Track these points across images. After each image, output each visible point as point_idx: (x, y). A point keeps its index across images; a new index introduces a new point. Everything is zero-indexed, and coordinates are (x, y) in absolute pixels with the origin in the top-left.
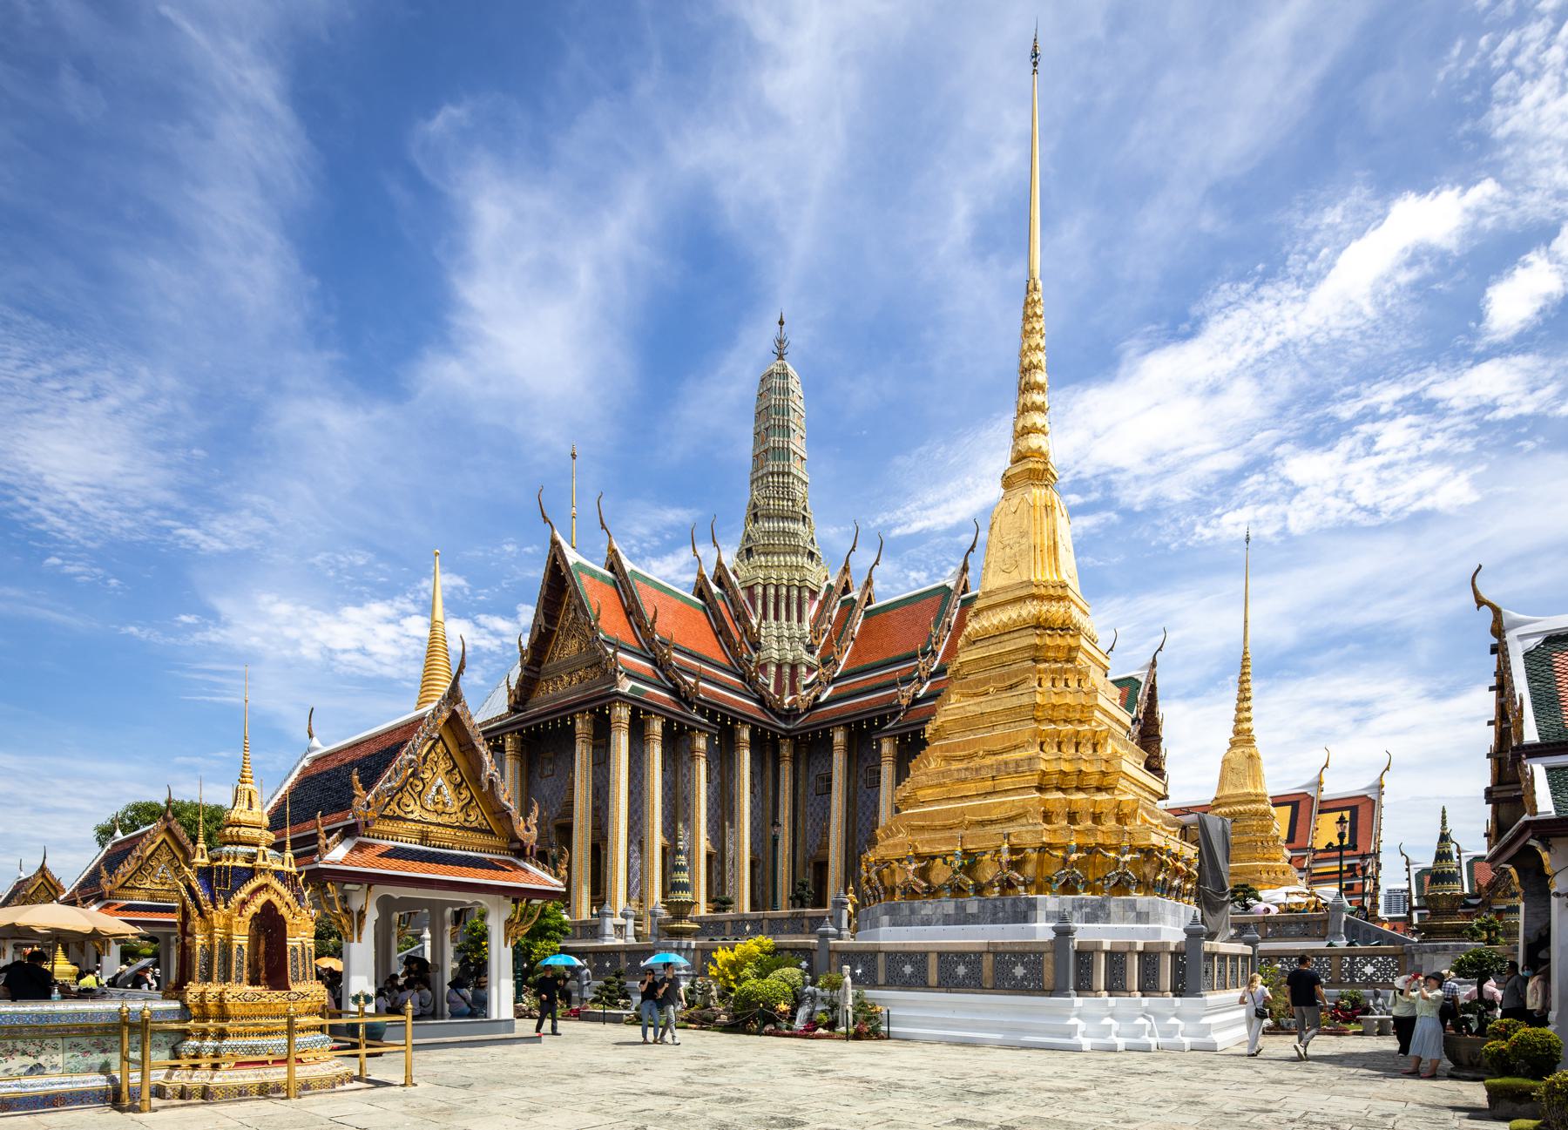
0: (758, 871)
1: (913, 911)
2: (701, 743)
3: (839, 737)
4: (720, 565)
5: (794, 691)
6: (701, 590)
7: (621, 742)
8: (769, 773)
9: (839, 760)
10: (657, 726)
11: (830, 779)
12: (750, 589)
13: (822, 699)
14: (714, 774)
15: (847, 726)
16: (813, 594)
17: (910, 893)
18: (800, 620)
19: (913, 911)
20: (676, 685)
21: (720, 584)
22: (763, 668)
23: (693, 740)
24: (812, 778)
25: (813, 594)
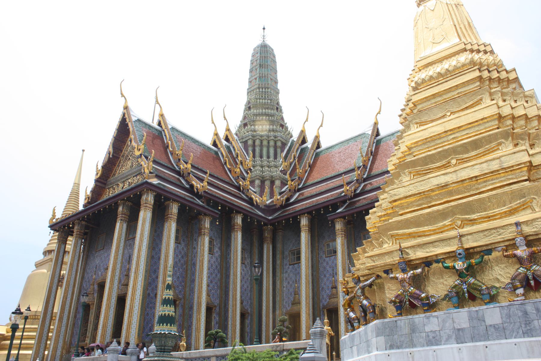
0: (247, 322)
1: (413, 329)
2: (207, 224)
3: (304, 222)
4: (228, 130)
5: (272, 195)
6: (215, 142)
7: (145, 216)
8: (256, 251)
9: (304, 237)
10: (174, 209)
11: (299, 253)
13: (292, 201)
14: (216, 249)
15: (308, 213)
16: (282, 143)
17: (406, 305)
18: (275, 157)
19: (413, 329)
20: (192, 186)
21: (227, 139)
22: (252, 182)
23: (200, 221)
24: (286, 253)
25: (284, 145)
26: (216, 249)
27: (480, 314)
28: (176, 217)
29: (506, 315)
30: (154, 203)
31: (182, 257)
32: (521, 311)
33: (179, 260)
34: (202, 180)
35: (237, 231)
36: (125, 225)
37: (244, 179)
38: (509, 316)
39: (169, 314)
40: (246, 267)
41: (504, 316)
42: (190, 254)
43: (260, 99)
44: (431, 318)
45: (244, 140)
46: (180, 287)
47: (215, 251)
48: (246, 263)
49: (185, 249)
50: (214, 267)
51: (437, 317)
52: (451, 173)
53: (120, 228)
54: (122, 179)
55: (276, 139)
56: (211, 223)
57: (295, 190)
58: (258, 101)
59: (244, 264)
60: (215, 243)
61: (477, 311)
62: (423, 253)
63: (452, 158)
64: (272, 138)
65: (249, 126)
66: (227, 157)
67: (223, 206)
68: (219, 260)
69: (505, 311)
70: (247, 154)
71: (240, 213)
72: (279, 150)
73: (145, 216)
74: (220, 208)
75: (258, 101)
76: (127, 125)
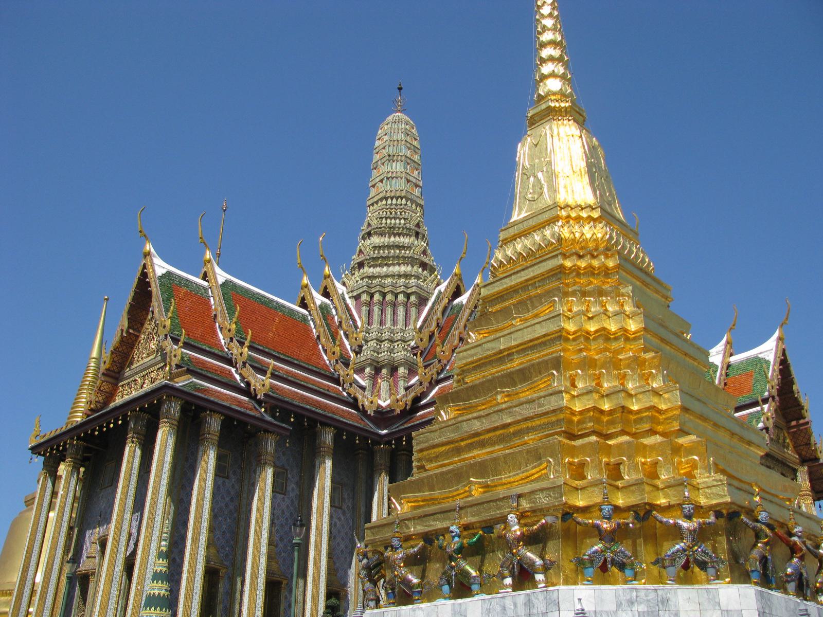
10: (214, 424)
12: (357, 298)
26: (292, 486)
27: (463, 608)
28: (216, 438)
29: (487, 610)
30: (180, 418)
31: (232, 500)
32: (500, 605)
33: (227, 505)
34: (263, 372)
35: (324, 456)
36: (138, 452)
37: (347, 365)
38: (489, 610)
39: (159, 594)
40: (344, 513)
41: (484, 611)
42: (245, 495)
43: (386, 218)
44: (417, 610)
45: (355, 294)
46: (227, 549)
47: (289, 488)
48: (345, 507)
49: (237, 487)
50: (287, 514)
51: (423, 610)
52: (483, 416)
53: (131, 453)
54: (141, 371)
55: (409, 291)
56: (278, 445)
57: (430, 383)
58: (384, 221)
59: (340, 508)
60: (289, 476)
61: (460, 604)
62: (422, 528)
63: (497, 393)
64: (402, 289)
65: (366, 268)
66: (322, 326)
67: (300, 417)
68: (296, 503)
69: (486, 606)
70: (360, 317)
71: (329, 425)
72: (413, 311)
73: (165, 440)
74: (292, 420)
75: (384, 221)
76: (148, 284)
